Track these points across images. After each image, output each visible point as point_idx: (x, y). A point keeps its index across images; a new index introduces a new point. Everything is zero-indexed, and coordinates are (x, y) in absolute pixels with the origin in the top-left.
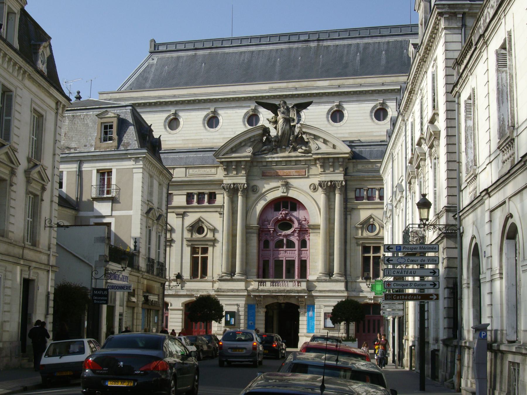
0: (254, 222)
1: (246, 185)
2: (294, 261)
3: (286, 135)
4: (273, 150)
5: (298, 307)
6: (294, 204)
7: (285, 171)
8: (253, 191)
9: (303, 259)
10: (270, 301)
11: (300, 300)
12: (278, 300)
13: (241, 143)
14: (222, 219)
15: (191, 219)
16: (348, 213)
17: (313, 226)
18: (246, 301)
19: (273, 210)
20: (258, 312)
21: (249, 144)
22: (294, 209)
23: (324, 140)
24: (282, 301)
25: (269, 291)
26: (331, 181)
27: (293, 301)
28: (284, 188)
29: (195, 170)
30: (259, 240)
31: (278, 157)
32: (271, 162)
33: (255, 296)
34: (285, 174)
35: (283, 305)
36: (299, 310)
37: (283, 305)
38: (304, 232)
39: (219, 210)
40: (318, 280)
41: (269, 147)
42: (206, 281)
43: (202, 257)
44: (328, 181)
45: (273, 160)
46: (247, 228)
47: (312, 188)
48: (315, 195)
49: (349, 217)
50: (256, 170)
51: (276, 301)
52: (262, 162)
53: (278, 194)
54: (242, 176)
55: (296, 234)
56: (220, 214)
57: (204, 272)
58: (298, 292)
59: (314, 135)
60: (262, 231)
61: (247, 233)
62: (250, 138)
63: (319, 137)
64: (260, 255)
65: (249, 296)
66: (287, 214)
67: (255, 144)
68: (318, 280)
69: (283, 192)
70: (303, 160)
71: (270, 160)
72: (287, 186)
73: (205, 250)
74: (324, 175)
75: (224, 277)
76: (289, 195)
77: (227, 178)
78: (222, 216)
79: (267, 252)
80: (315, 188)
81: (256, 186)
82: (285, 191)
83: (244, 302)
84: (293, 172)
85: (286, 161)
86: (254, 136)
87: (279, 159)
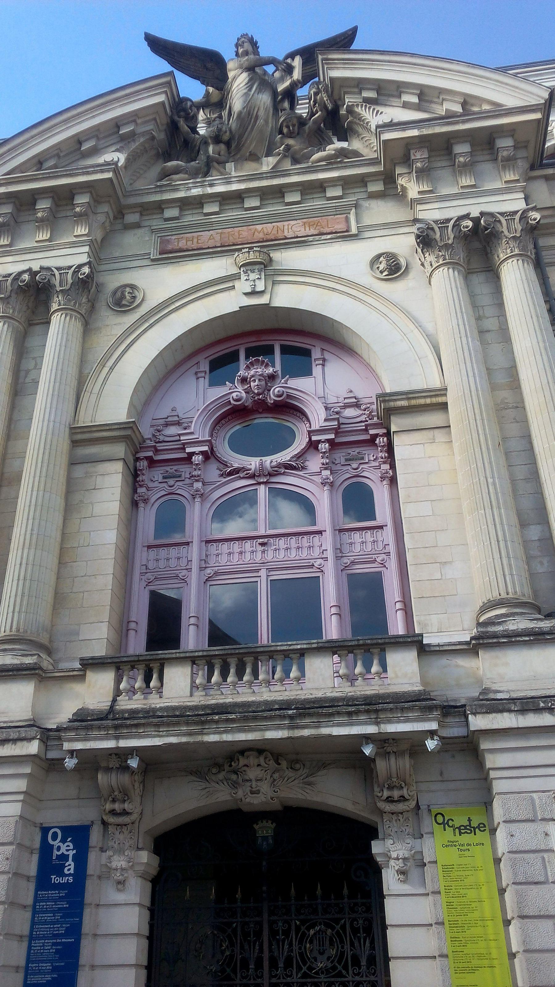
0: (113, 404)
1: (86, 270)
2: (310, 588)
3: (261, 122)
5: (371, 832)
6: (298, 339)
7: (259, 227)
8: (118, 303)
9: (359, 569)
10: (185, 800)
11: (381, 765)
12: (235, 785)
13: (78, 140)
17: (408, 395)
18: (30, 798)
19: (203, 383)
20: (106, 873)
22: (299, 359)
24: (262, 791)
25: (176, 717)
27: (336, 794)
28: (253, 276)
30: (134, 502)
33: (91, 763)
34: (261, 236)
35: (265, 830)
36: (376, 848)
37: (265, 830)
38: (354, 451)
40: (486, 640)
45: (210, 190)
46: (83, 441)
48: (396, 290)
50: (137, 241)
52: (160, 207)
53: (228, 303)
54: (73, 245)
55: (315, 463)
58: (372, 706)
61: (73, 463)
65: (48, 766)
66: (272, 377)
67: (133, 146)
68: (486, 640)
69: (253, 293)
70: (333, 182)
72: (265, 266)
74: (436, 205)
76: (278, 302)
79: (173, 552)
81: (133, 287)
82: (260, 286)
83: (14, 809)
84: (295, 228)
86: (133, 117)
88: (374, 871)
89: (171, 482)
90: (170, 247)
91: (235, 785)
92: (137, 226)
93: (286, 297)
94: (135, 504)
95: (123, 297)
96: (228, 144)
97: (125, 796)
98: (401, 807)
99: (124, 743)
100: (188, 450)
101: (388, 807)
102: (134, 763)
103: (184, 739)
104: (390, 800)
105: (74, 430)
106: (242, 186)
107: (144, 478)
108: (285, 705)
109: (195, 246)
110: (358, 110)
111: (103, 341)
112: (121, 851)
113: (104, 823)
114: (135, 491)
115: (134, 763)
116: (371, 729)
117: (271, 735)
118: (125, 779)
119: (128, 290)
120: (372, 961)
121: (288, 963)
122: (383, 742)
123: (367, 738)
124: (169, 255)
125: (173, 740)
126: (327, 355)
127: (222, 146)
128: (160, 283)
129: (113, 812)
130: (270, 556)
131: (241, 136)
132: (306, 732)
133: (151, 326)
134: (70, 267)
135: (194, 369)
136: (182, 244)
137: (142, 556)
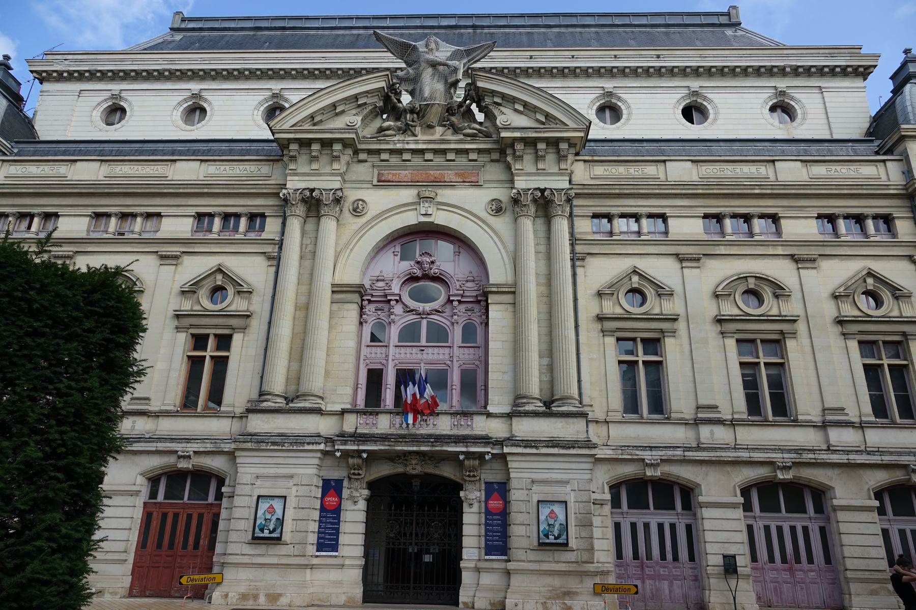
4: (406, 130)
5: (460, 487)
7: (432, 172)
10: (383, 470)
11: (466, 462)
14: (273, 269)
15: (195, 266)
16: (578, 263)
21: (354, 112)
23: (526, 104)
24: (415, 468)
25: (384, 438)
26: (542, 191)
27: (447, 471)
28: (427, 205)
29: (222, 168)
31: (417, 142)
32: (400, 152)
33: (346, 454)
35: (416, 483)
36: (462, 494)
37: (416, 483)
39: (269, 249)
41: (399, 124)
42: (217, 415)
43: (212, 357)
44: (535, 189)
45: (407, 147)
47: (494, 207)
49: (579, 271)
51: (400, 469)
52: (378, 152)
53: (411, 219)
56: (269, 258)
57: (216, 395)
59: (503, 96)
60: (370, 301)
62: (356, 97)
63: (513, 100)
64: (362, 358)
67: (366, 111)
70: (473, 150)
71: (399, 146)
73: (224, 342)
74: (524, 178)
75: (265, 404)
77: (296, 178)
78: (275, 263)
80: (501, 209)
85: (436, 152)
87: (421, 146)
88: (460, 502)
89: (379, 312)
90: (383, 178)
91: (406, 465)
92: (366, 161)
93: (441, 218)
94: (361, 323)
95: (358, 207)
96: (418, 114)
97: (359, 468)
98: (473, 479)
99: (361, 448)
100: (389, 298)
101: (468, 479)
102: (365, 455)
103: (387, 448)
104: (469, 476)
105: (333, 285)
106: (424, 147)
107: (366, 310)
108: (430, 436)
109: (397, 180)
110: (491, 107)
111: (348, 232)
112: (357, 490)
113: (350, 478)
114: (361, 316)
115: (365, 455)
116: (464, 449)
117: (423, 448)
118: (360, 461)
119: (361, 203)
120: (456, 535)
121: (422, 535)
122: (469, 455)
123: (463, 453)
124: (383, 183)
125: (383, 448)
126: (461, 250)
127: (415, 116)
128: (378, 200)
129: (354, 474)
130: (425, 356)
131: (425, 110)
132: (437, 448)
133: (372, 227)
134: (331, 190)
135: (393, 250)
136: (390, 177)
137: (365, 351)
